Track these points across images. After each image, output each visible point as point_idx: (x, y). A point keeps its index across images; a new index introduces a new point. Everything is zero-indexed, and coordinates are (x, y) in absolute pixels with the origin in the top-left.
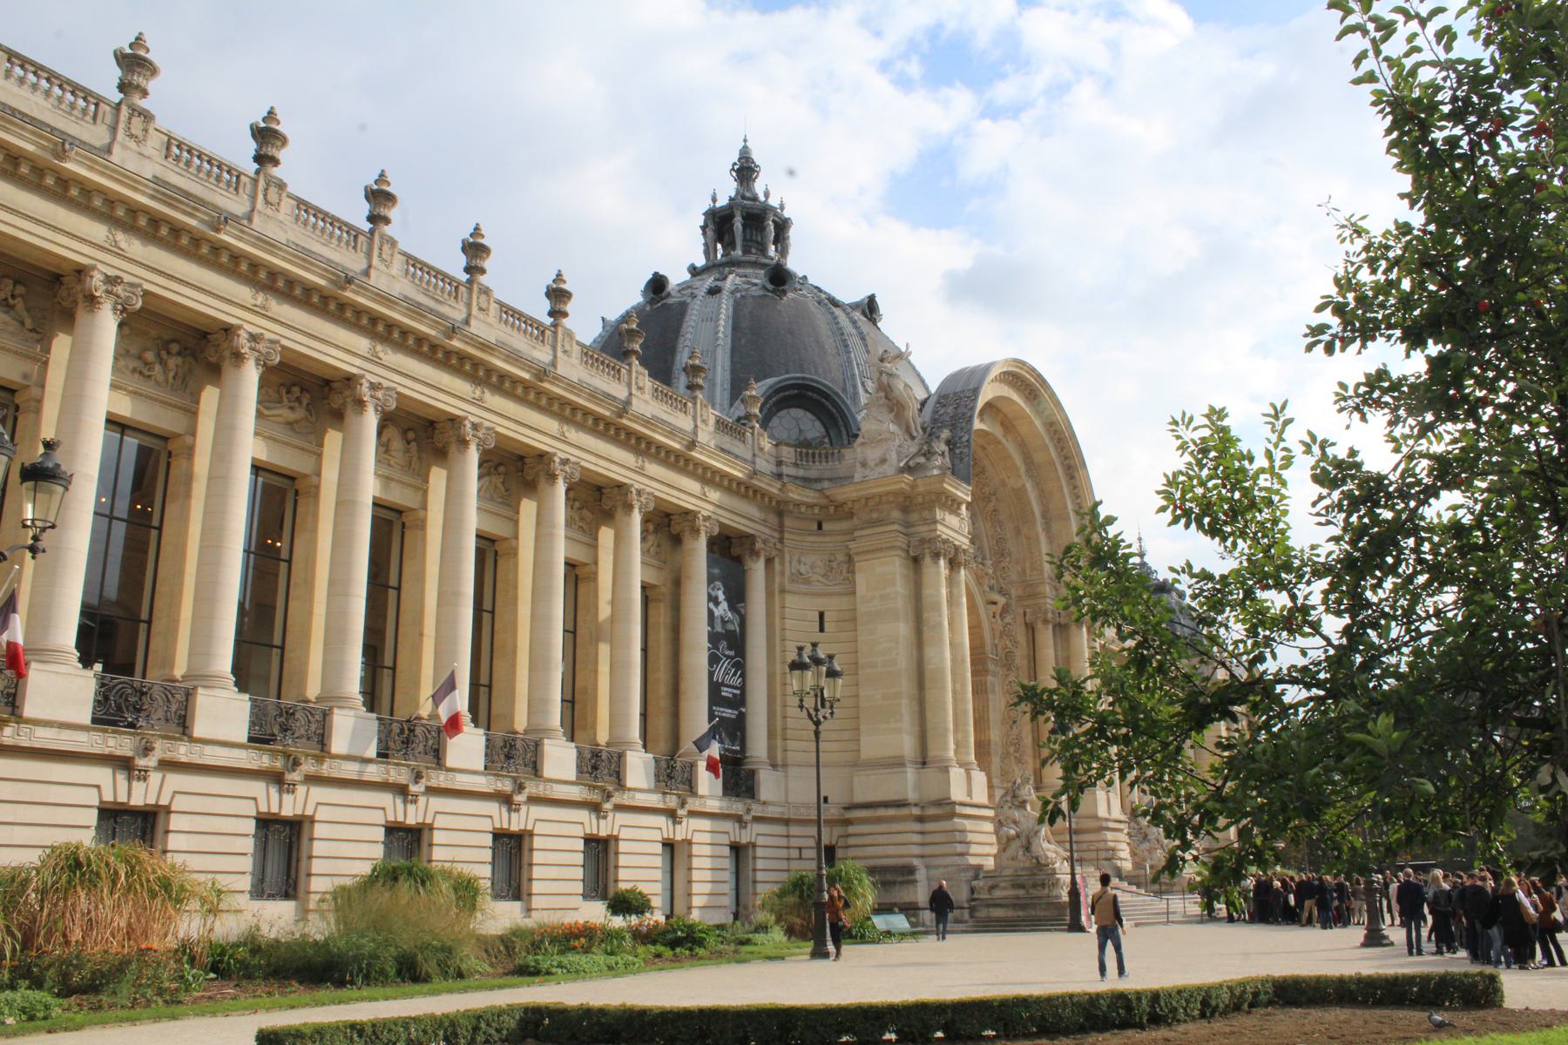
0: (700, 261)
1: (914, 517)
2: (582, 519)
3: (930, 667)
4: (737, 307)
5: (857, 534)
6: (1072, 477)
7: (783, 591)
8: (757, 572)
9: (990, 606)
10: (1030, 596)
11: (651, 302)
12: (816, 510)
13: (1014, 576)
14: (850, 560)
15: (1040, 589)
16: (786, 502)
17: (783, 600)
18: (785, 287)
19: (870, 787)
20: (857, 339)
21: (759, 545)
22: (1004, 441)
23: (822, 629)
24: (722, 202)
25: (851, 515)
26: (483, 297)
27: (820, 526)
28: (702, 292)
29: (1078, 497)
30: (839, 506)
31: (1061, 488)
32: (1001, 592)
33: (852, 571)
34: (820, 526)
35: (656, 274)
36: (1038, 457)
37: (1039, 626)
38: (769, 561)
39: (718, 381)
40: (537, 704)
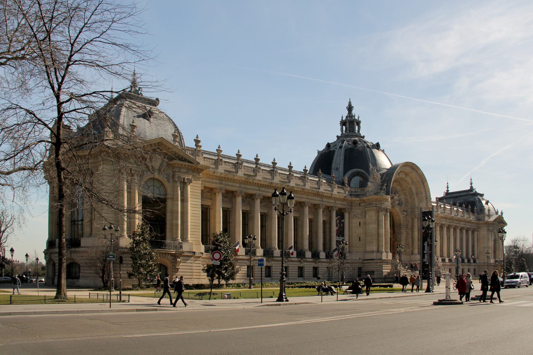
0: (339, 135)
5: (367, 206)
6: (423, 184)
8: (346, 215)
10: (413, 212)
11: (328, 149)
13: (410, 207)
15: (415, 210)
16: (353, 200)
18: (356, 145)
19: (368, 256)
23: (360, 226)
24: (344, 119)
25: (366, 202)
27: (360, 205)
28: (338, 147)
30: (363, 200)
32: (406, 211)
33: (366, 214)
34: (360, 205)
35: (328, 143)
37: (414, 218)
38: (349, 213)
39: (341, 171)
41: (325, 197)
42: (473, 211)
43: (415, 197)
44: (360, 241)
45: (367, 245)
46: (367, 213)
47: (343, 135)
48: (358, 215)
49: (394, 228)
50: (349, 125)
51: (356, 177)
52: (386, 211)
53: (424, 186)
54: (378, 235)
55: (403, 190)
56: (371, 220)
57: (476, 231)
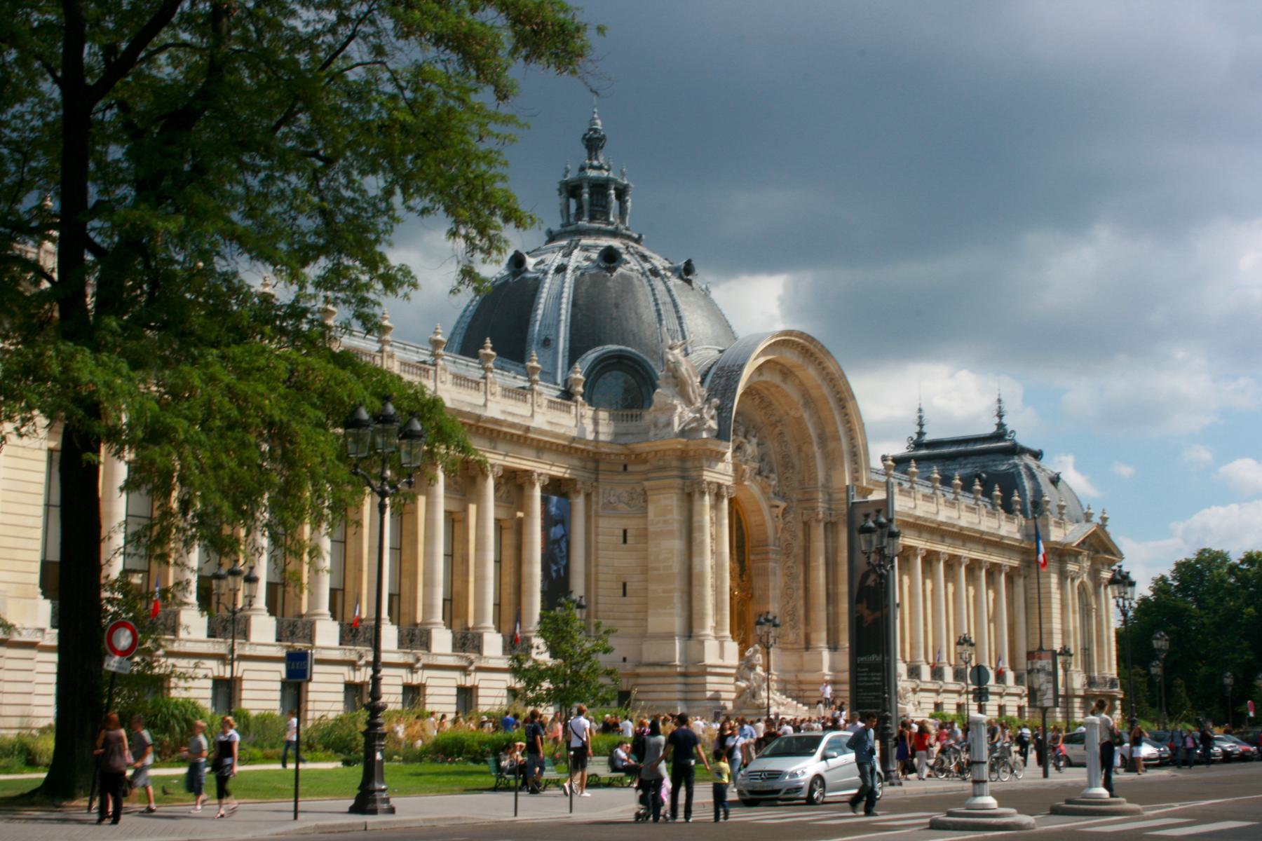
0: (556, 227)
1: (689, 464)
2: (456, 483)
3: (696, 570)
4: (577, 283)
5: (650, 475)
6: (844, 407)
7: (597, 516)
9: (774, 509)
10: (808, 500)
12: (622, 457)
14: (645, 493)
16: (600, 453)
17: (597, 522)
20: (670, 307)
21: (579, 486)
22: (783, 385)
23: (625, 541)
25: (645, 461)
26: (390, 360)
29: (849, 422)
31: (833, 417)
32: (784, 497)
33: (646, 501)
34: (625, 467)
36: (814, 393)
37: (813, 524)
38: (588, 496)
40: (429, 609)
41: (504, 438)
42: (1008, 508)
43: (816, 448)
44: (625, 594)
45: (650, 611)
46: (650, 498)
47: (569, 228)
48: (622, 505)
49: (743, 552)
50: (591, 195)
51: (614, 373)
52: (718, 496)
53: (846, 415)
54: (690, 579)
55: (775, 425)
56: (665, 522)
57: (1020, 576)
